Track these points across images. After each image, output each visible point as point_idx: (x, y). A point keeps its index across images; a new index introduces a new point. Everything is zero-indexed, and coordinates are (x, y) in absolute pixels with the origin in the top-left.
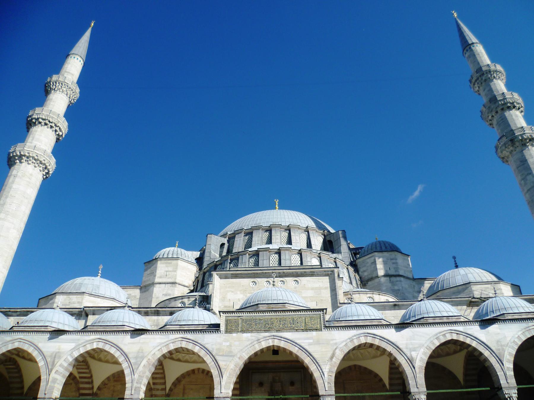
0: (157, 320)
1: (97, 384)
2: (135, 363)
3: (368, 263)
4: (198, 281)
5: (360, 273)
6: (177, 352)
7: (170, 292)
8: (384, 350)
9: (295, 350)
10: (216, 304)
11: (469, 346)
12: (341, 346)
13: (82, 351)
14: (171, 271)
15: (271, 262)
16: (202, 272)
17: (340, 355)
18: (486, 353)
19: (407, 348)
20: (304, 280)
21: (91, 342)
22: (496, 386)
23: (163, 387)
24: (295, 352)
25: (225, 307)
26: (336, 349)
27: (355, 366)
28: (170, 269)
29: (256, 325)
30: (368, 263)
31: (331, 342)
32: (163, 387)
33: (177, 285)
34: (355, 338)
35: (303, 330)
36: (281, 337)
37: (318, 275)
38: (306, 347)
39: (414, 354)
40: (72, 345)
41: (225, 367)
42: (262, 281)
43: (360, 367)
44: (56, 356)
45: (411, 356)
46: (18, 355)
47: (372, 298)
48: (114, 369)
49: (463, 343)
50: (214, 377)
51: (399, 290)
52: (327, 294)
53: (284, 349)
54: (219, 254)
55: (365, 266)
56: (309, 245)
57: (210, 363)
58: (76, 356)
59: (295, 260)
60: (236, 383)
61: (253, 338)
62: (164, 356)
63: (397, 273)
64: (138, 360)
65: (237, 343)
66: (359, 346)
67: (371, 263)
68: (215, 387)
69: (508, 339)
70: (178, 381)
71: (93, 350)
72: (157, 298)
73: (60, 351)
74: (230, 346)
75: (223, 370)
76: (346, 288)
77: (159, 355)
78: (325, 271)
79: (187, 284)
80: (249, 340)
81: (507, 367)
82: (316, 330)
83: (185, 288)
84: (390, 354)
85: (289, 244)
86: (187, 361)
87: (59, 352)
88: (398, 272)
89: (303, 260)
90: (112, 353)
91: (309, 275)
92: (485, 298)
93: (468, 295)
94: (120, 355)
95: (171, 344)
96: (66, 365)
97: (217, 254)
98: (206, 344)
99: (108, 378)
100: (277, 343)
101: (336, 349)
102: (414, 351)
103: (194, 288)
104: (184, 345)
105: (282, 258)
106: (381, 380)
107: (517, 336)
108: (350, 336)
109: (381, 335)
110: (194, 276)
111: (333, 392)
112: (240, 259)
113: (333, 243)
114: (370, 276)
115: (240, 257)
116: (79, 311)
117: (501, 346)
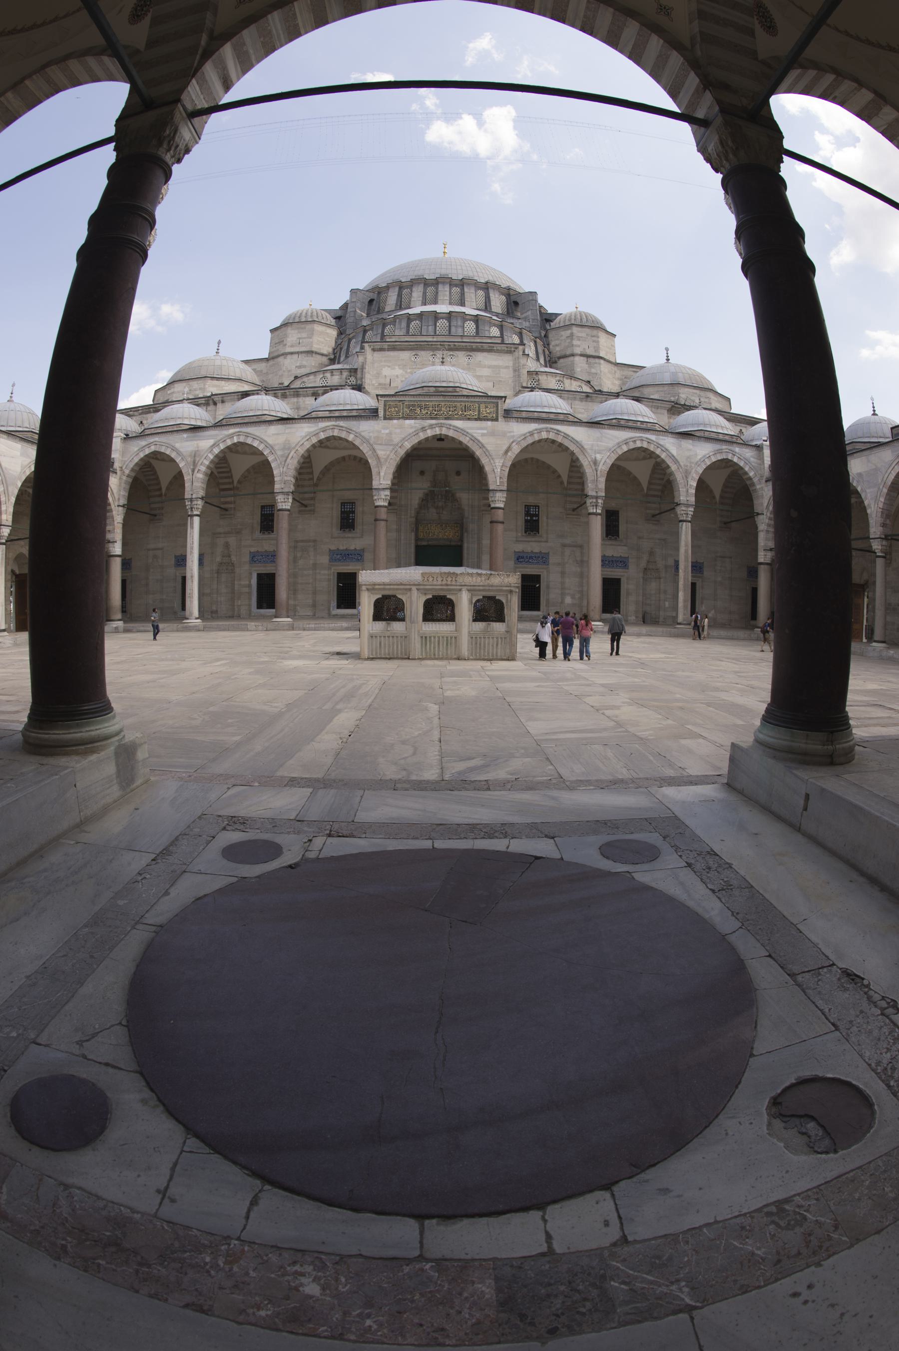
0: (297, 402)
1: (236, 477)
2: (282, 456)
3: (562, 336)
4: (341, 349)
5: (551, 347)
6: (328, 441)
7: (304, 363)
8: (567, 449)
9: (465, 440)
10: (369, 381)
11: (659, 456)
12: (519, 439)
13: (222, 446)
14: (305, 338)
15: (438, 328)
16: (346, 339)
17: (516, 449)
18: (673, 467)
19: (592, 450)
20: (480, 357)
21: (231, 436)
22: (676, 501)
23: (311, 476)
24: (466, 443)
25: (380, 384)
26: (513, 442)
27: (532, 459)
28: (304, 335)
29: (421, 411)
30: (562, 336)
31: (509, 434)
32: (311, 476)
33: (314, 355)
34: (536, 432)
35: (476, 420)
36: (450, 425)
37: (498, 351)
38: (480, 438)
39: (598, 457)
40: (211, 442)
41: (385, 457)
42: (425, 355)
43: (538, 460)
44: (195, 454)
45: (595, 459)
46: (153, 458)
47: (562, 382)
48: (256, 460)
49: (653, 453)
50: (371, 467)
51: (596, 374)
52: (507, 375)
53: (453, 439)
54: (366, 312)
55: (558, 339)
56: (487, 307)
57: (367, 452)
58: (217, 453)
59: (470, 326)
60: (394, 473)
61: (417, 425)
62: (314, 446)
63: (597, 354)
64: (286, 452)
65: (398, 431)
66: (540, 441)
67: (567, 337)
68: (374, 477)
69: (699, 457)
70: (327, 469)
71: (234, 444)
72: (289, 371)
73: (199, 449)
74: (390, 433)
75: (382, 460)
76: (531, 365)
77: (308, 445)
78: (507, 347)
79: (325, 352)
80: (412, 428)
81: (690, 485)
82: (492, 420)
83: (324, 357)
84: (573, 453)
85: (462, 306)
86: (335, 448)
87: (198, 450)
88: (599, 352)
89: (480, 327)
90: (255, 446)
91: (487, 350)
92: (688, 406)
93: (674, 396)
94: (264, 448)
95: (322, 433)
96: (207, 463)
97: (364, 312)
98: (362, 431)
99: (248, 471)
100: (444, 431)
101: (513, 442)
102: (599, 453)
103: (335, 357)
104: (336, 433)
105: (452, 324)
106: (559, 476)
107: (708, 456)
108: (531, 430)
109: (565, 432)
110: (334, 342)
111: (505, 488)
112: (397, 323)
113: (520, 306)
114: (563, 353)
115: (397, 320)
116: (205, 400)
117: (691, 463)
